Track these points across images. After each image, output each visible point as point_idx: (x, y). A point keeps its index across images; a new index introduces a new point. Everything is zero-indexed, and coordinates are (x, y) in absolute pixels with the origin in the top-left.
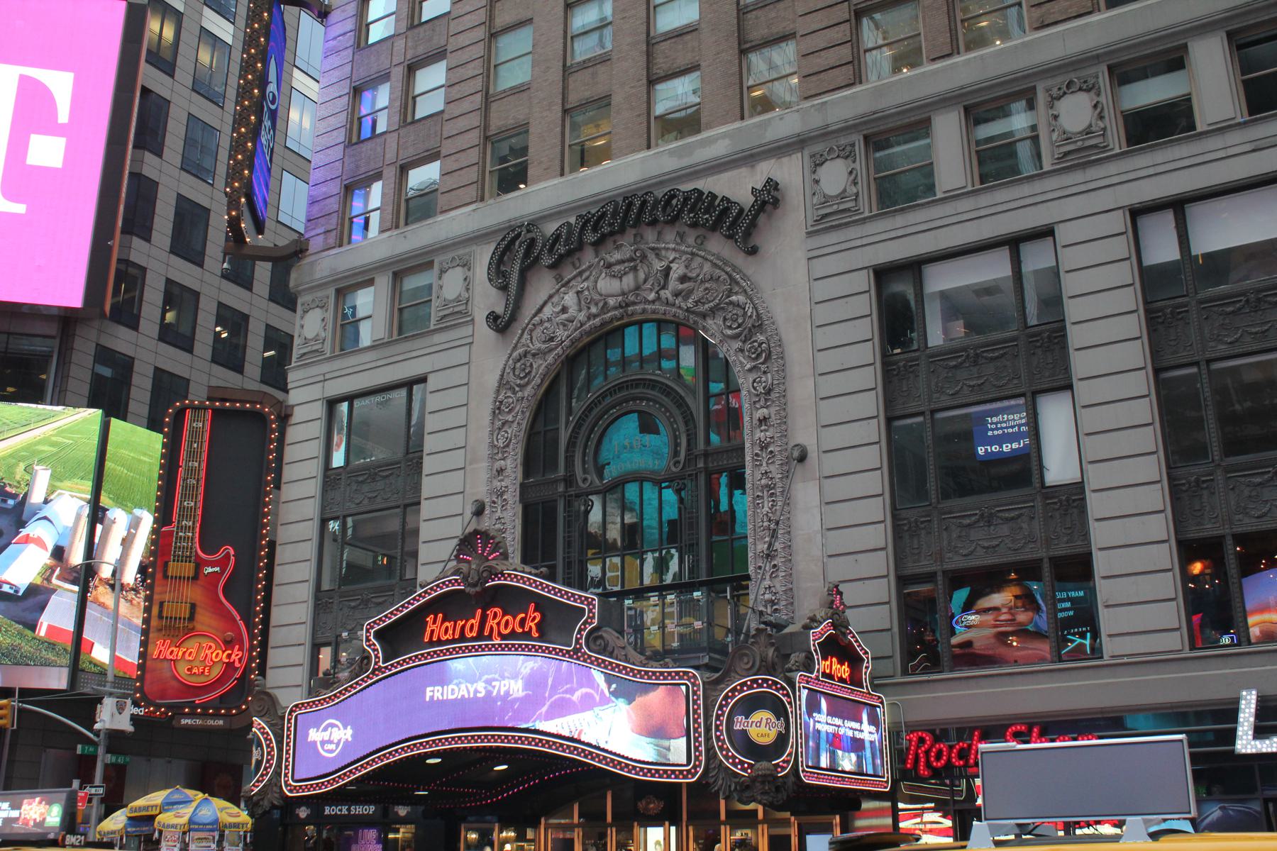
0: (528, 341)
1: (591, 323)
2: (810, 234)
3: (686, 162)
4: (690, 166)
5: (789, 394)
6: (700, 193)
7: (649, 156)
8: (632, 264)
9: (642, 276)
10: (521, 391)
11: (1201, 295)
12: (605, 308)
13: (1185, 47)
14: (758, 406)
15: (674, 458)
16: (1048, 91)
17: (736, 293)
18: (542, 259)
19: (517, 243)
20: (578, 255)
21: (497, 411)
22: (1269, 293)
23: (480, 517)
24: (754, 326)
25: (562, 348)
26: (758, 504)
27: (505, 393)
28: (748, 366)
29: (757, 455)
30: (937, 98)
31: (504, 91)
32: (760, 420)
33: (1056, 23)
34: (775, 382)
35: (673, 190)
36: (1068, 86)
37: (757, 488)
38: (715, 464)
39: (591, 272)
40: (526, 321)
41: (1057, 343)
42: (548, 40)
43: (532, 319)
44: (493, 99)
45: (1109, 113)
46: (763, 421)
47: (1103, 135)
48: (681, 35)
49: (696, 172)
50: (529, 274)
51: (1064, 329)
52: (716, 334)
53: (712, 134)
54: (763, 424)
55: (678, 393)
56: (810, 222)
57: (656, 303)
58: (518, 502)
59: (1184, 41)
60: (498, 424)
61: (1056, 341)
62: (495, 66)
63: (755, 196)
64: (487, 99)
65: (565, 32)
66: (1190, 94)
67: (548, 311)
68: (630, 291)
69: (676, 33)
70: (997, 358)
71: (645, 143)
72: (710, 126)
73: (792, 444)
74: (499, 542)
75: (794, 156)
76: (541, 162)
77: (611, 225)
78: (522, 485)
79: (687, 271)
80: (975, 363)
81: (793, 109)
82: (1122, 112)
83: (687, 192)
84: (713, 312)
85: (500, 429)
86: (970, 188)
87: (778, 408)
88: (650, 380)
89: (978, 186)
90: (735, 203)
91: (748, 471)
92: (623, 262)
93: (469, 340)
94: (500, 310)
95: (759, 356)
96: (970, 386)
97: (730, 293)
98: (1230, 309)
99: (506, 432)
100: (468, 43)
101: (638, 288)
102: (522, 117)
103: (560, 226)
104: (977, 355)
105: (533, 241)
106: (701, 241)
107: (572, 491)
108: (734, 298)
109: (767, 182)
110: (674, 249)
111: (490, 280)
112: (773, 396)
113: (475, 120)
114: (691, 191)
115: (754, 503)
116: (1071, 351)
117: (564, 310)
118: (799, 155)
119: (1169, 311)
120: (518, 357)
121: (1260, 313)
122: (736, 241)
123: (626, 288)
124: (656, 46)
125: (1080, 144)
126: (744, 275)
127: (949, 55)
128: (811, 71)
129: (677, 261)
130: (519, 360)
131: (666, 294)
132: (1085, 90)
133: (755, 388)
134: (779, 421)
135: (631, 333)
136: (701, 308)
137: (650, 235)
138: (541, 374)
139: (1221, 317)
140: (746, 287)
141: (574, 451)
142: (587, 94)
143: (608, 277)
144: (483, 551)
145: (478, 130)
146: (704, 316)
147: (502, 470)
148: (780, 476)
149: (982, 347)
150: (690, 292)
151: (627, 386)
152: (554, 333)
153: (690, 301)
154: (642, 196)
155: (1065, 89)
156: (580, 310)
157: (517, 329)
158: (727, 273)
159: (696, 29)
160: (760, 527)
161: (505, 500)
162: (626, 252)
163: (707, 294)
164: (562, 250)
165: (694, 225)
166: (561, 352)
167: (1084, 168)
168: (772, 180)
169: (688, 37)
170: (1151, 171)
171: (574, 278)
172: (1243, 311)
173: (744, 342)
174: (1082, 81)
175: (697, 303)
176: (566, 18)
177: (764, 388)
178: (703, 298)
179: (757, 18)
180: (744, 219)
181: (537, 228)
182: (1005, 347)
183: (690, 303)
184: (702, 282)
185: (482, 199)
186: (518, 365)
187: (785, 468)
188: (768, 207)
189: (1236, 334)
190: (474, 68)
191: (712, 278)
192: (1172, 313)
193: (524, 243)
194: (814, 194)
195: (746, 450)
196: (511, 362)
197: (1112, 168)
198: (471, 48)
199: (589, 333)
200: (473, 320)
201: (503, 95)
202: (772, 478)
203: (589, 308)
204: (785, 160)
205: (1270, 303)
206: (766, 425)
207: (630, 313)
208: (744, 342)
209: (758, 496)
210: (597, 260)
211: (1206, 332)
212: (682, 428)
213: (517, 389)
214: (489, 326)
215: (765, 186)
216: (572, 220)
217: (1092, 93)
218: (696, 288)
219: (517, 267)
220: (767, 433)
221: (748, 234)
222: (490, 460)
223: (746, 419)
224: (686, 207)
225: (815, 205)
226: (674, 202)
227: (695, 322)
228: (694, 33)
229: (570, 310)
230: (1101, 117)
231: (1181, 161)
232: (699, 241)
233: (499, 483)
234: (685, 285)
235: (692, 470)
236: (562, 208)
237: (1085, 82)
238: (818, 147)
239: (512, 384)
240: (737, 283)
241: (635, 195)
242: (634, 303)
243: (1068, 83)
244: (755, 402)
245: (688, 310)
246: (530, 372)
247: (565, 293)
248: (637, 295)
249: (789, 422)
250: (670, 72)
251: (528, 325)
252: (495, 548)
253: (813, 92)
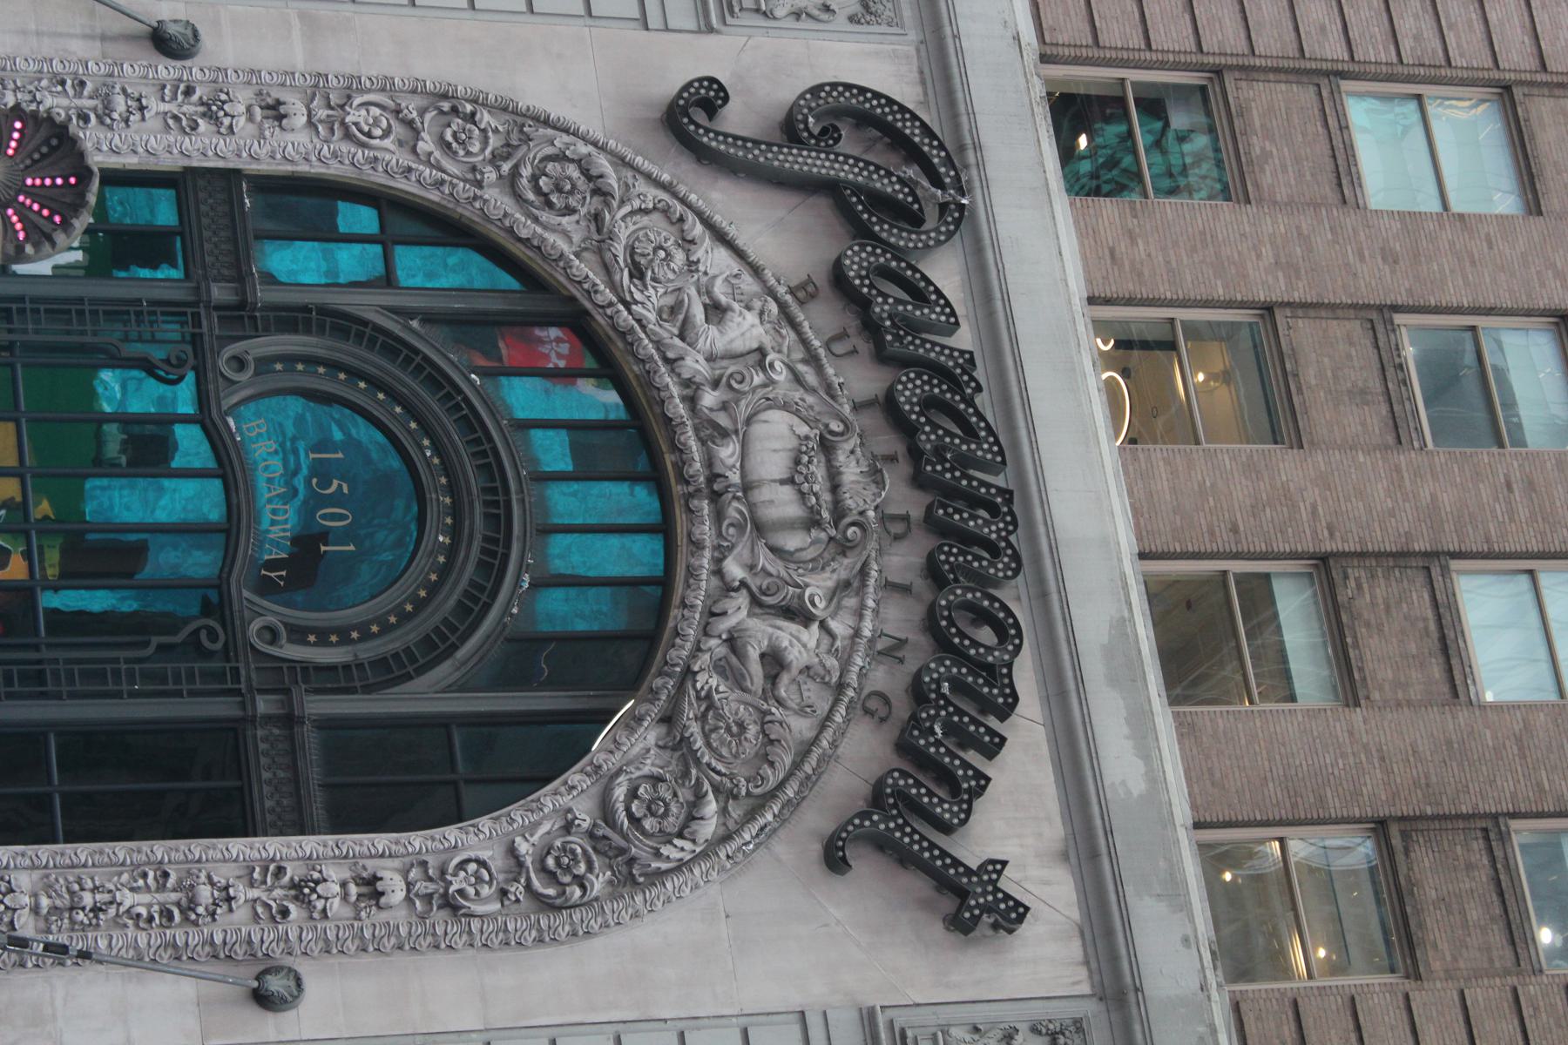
0: (636, 204)
1: (675, 390)
2: (868, 1018)
3: (1094, 667)
4: (1080, 680)
5: (442, 958)
6: (1006, 711)
7: (1120, 560)
8: (826, 515)
9: (793, 541)
10: (500, 177)
12: (713, 433)
14: (413, 874)
15: (285, 624)
17: (724, 812)
18: (863, 247)
19: (911, 172)
20: (864, 347)
21: (446, 106)
23: (148, 44)
24: (632, 861)
25: (611, 304)
26: (145, 876)
27: (496, 131)
28: (523, 847)
29: (280, 870)
31: (1344, 127)
32: (375, 879)
34: (475, 925)
35: (1019, 635)
37: (189, 872)
38: (262, 746)
39: (813, 391)
40: (693, 197)
42: (1473, 263)
43: (699, 214)
44: (1325, 93)
46: (372, 889)
48: (1445, 649)
49: (1063, 694)
50: (822, 204)
52: (618, 755)
53: (1164, 744)
54: (364, 890)
55: (464, 638)
56: (901, 1018)
57: (715, 581)
58: (186, 163)
60: (411, 107)
62: (1419, 97)
63: (982, 867)
64: (1327, 74)
65: (1490, 311)
67: (716, 260)
68: (752, 507)
69: (1450, 634)
71: (1158, 545)
72: (1186, 731)
73: (303, 967)
74: (53, 244)
75: (1083, 973)
77: (939, 451)
78: (237, 173)
79: (794, 671)
81: (1210, 973)
83: (1010, 675)
84: (679, 746)
85: (398, 112)
87: (403, 931)
88: (506, 557)
90: (968, 812)
91: (236, 846)
92: (835, 488)
93: (654, 19)
94: (736, 118)
95: (551, 877)
97: (726, 795)
99: (387, 133)
100: (1493, 17)
101: (760, 528)
102: (1267, 179)
103: (948, 304)
105: (916, 220)
106: (874, 707)
107: (210, 325)
108: (711, 807)
109: (1018, 904)
110: (857, 633)
111: (815, 90)
112: (439, 916)
113: (1272, 41)
114: (1011, 685)
115: (149, 863)
117: (716, 311)
118: (1085, 989)
120: (594, 172)
122: (864, 815)
123: (762, 495)
124: (1420, 579)
126: (774, 831)
128: (1308, 1022)
129: (826, 641)
130: (586, 173)
131: (738, 611)
133: (462, 865)
134: (368, 934)
135: (636, 501)
136: (690, 711)
137: (904, 560)
138: (544, 240)
140: (738, 841)
141: (321, 331)
142: (1310, 375)
143: (794, 443)
144: (31, 192)
145: (1242, 46)
146: (668, 720)
147: (281, 117)
148: (218, 939)
150: (737, 680)
151: (493, 491)
152: (654, 279)
153: (714, 682)
154: (1009, 545)
156: (710, 359)
157: (674, 167)
158: (781, 785)
159: (1456, 695)
160: (79, 881)
161: (194, 127)
162: (858, 493)
163: (728, 729)
164: (880, 308)
165: (918, 692)
166: (599, 299)
168: (1021, 918)
169: (1437, 671)
171: (804, 342)
173: (591, 835)
175: (707, 697)
176: (1528, 313)
177: (461, 892)
178: (719, 717)
179: (1470, 867)
180: (923, 838)
181: (950, 235)
183: (708, 680)
184: (764, 717)
185: (1044, 59)
186: (573, 171)
187: (240, 951)
188: (948, 904)
190: (1417, 38)
191: (772, 742)
193: (912, 193)
194: (976, 1030)
195: (294, 840)
196: (583, 149)
198: (1478, 27)
199: (648, 380)
200: (711, 30)
201: (1332, 122)
202: (213, 914)
203: (715, 384)
204: (1075, 949)
206: (360, 895)
207: (694, 503)
208: (591, 835)
209: (166, 875)
210: (847, 409)
212: (367, 651)
213: (506, 167)
214: (690, 84)
215: (1007, 897)
216: (964, 338)
218: (747, 697)
219: (846, 173)
220: (337, 901)
221: (882, 844)
222: (310, 81)
223: (382, 841)
224: (970, 672)
225: (945, 1033)
226: (986, 635)
227: (654, 694)
228: (1445, 689)
229: (713, 331)
232: (873, 704)
233: (242, 108)
234: (756, 669)
235: (249, 678)
236: (999, 304)
239: (519, 154)
240: (750, 816)
241: (1015, 522)
242: (719, 516)
244: (424, 864)
245: (689, 673)
246: (549, 205)
247: (761, 313)
248: (740, 527)
249: (365, 959)
250: (1344, 618)
251: (683, 201)
252: (36, 227)
253: (1251, 1027)
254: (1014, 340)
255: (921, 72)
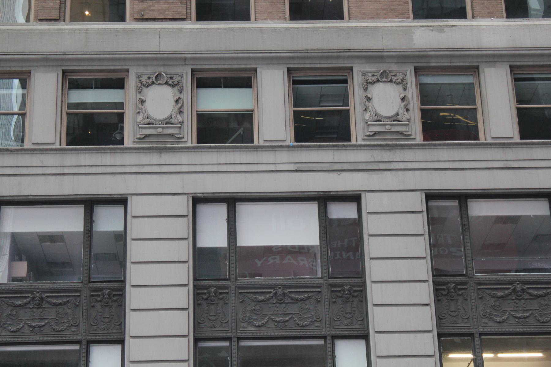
11: (242, 281)
13: (255, 70)
16: (139, 77)
22: (293, 290)
30: (41, 56)
33: (154, 20)
36: (156, 77)
41: (115, 301)
45: (187, 109)
47: (180, 128)
51: (123, 289)
61: (115, 298)
66: (253, 111)
70: (60, 304)
80: (39, 306)
82: (197, 111)
86: (57, 146)
89: (64, 146)
96: (31, 326)
98: (261, 298)
104: (42, 299)
116: (127, 310)
119: (213, 290)
121: (284, 305)
125: (160, 130)
127: (56, 20)
132: (170, 85)
139: (254, 303)
149: (48, 292)
155: (154, 79)
167: (160, 152)
170: (215, 168)
172: (271, 301)
174: (169, 76)
182: (69, 296)
189: (264, 319)
192: (215, 292)
197: (184, 158)
205: (292, 299)
211: (240, 313)
217: (176, 89)
230: (181, 112)
231: (240, 166)
237: (171, 78)
243: (157, 76)
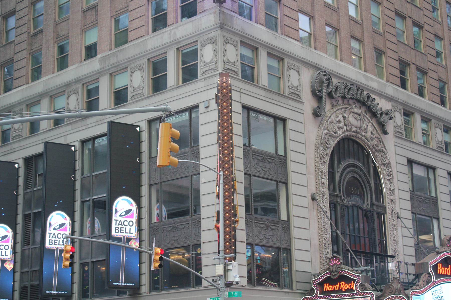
4: (368, 86)
12: (351, 130)
46: (392, 200)
59: (413, 111)
76: (320, 42)
146: (376, 151)
162: (359, 111)
204: (387, 102)
213: (326, 149)
238: (394, 104)
254: (337, 73)
255: (305, 67)
